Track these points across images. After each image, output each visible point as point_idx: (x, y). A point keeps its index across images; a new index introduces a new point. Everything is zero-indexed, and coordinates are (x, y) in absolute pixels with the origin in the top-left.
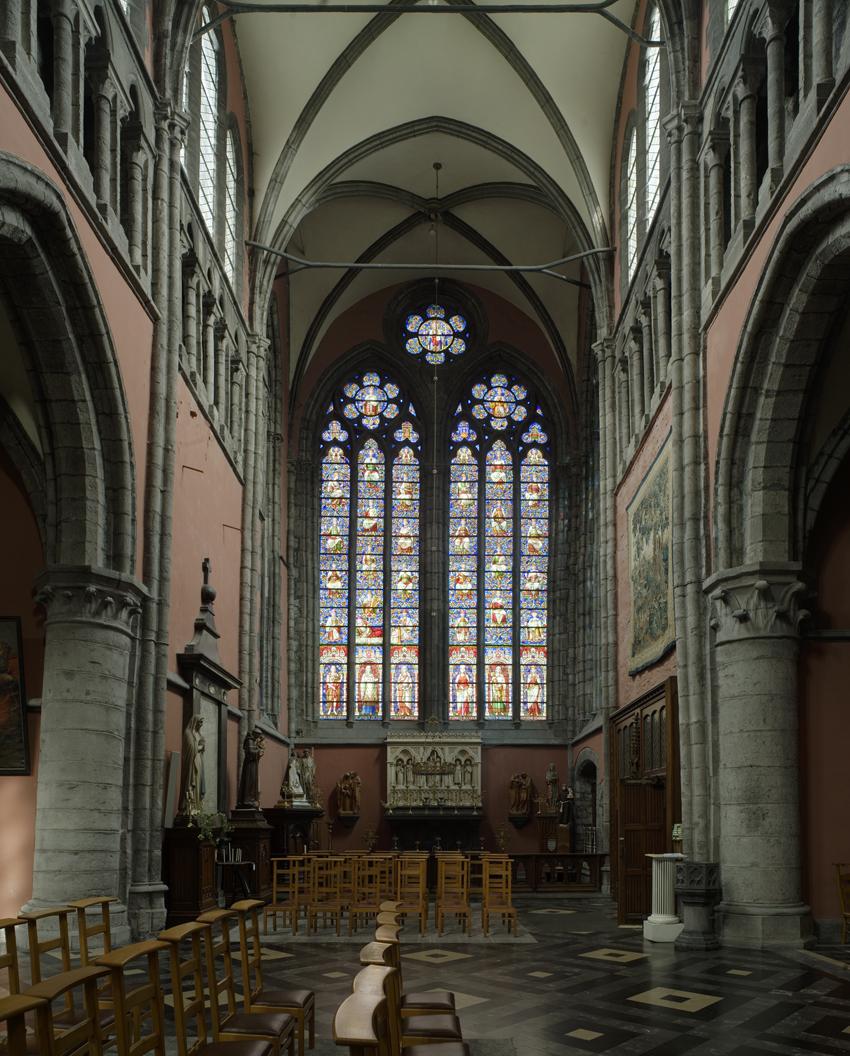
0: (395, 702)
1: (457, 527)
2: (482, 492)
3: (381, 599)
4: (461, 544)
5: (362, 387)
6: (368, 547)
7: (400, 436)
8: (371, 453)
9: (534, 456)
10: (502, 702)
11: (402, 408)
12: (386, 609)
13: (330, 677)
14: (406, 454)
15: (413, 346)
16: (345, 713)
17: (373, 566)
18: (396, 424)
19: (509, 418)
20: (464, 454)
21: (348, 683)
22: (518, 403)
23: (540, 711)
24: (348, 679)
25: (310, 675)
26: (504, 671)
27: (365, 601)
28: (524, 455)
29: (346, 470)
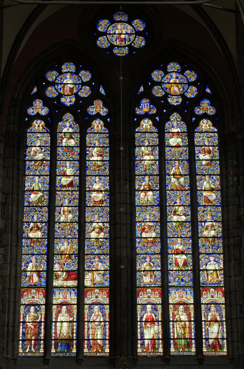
0: (89, 340)
1: (142, 183)
2: (162, 154)
3: (76, 247)
4: (146, 197)
5: (61, 73)
6: (66, 201)
7: (92, 110)
8: (68, 124)
9: (205, 125)
10: (185, 339)
11: (92, 88)
12: (81, 255)
13: (30, 317)
14: (98, 125)
15: (102, 42)
16: (42, 351)
17: (70, 216)
18: (89, 101)
19: (183, 96)
20: (146, 124)
21: (45, 322)
22: (190, 84)
23: (221, 347)
24: (46, 318)
25: (11, 315)
26: (186, 310)
27: (62, 248)
28: (197, 124)
29: (47, 138)
